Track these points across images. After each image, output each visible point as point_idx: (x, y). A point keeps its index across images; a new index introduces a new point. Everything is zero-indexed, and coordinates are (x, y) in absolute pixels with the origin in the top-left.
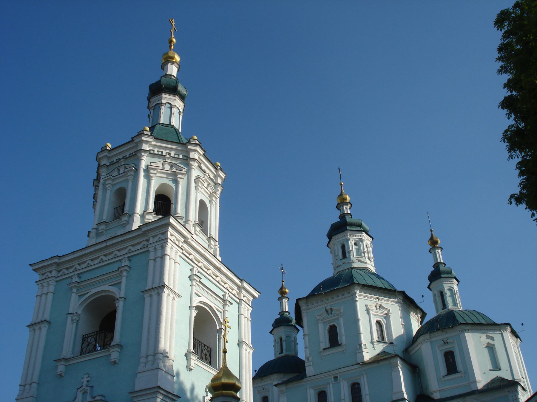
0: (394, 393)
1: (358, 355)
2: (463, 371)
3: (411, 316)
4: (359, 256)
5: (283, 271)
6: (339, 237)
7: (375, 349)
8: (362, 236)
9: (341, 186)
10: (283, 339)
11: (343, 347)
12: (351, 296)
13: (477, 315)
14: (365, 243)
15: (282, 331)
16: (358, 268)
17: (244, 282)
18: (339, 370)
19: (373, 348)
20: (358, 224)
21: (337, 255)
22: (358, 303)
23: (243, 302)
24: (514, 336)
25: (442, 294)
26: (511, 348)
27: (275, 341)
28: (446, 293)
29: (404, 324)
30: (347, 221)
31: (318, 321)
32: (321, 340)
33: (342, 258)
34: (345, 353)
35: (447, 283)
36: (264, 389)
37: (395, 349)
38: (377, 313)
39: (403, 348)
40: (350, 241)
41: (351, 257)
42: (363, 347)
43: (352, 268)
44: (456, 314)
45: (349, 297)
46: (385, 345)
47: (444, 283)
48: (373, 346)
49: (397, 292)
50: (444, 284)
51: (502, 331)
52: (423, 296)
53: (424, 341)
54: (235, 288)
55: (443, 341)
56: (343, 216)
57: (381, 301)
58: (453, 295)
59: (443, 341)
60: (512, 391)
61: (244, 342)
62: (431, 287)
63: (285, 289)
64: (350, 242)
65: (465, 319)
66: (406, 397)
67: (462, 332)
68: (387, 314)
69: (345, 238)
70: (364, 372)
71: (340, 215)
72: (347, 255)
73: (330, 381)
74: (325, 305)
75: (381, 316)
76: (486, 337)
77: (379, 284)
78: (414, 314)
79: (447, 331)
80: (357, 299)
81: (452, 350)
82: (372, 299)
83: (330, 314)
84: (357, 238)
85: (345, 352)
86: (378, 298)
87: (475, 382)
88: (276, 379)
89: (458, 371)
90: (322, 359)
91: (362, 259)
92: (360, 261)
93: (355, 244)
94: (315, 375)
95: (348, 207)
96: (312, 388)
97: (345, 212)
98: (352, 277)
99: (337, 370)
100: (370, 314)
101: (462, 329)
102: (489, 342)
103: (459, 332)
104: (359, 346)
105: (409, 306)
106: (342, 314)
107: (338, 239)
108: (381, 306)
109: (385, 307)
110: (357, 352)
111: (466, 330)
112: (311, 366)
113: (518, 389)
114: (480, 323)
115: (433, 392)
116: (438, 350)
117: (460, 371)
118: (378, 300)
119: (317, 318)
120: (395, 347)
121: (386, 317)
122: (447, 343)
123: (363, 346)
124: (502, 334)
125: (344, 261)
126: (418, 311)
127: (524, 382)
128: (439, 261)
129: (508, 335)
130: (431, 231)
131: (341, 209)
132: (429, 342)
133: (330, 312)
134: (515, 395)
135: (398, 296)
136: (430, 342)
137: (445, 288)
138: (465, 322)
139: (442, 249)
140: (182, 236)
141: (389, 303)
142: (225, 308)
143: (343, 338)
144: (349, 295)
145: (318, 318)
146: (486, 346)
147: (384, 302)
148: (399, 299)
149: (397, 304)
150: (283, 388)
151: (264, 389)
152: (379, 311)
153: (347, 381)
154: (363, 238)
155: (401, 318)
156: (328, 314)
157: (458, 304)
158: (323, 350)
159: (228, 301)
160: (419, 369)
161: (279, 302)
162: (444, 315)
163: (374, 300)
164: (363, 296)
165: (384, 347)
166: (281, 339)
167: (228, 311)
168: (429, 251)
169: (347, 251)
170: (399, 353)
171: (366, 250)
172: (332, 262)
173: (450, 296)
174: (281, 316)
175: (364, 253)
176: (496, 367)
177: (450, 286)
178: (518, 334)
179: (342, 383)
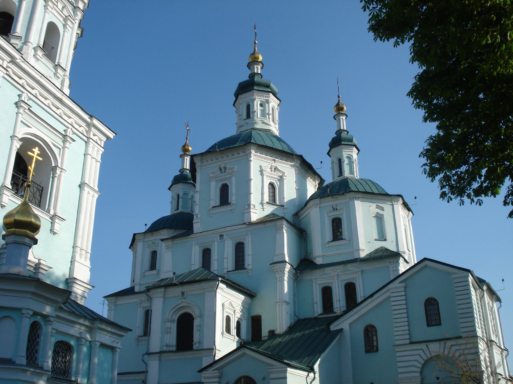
0: (276, 255)
1: (246, 215)
2: (348, 239)
3: (307, 181)
4: (264, 117)
5: (188, 128)
6: (246, 96)
7: (264, 210)
8: (269, 98)
9: (254, 45)
10: (180, 196)
11: (232, 206)
12: (245, 156)
13: (371, 185)
14: (271, 105)
15: (180, 188)
16: (260, 129)
17: (94, 118)
18: (225, 228)
19: (262, 209)
20: (266, 85)
21: (241, 115)
22: (252, 164)
23: (91, 140)
24: (406, 209)
25: (340, 161)
26: (400, 219)
27: (172, 197)
28: (344, 161)
29: (298, 188)
30: (255, 80)
32: (212, 198)
34: (233, 212)
35: (346, 150)
36: (154, 243)
37: (284, 212)
38: (271, 174)
39: (294, 212)
40: (256, 101)
42: (251, 208)
43: (254, 129)
44: (349, 181)
46: (276, 207)
47: (343, 150)
48: (262, 207)
49: (294, 155)
50: (343, 152)
51: (393, 202)
52: (321, 162)
53: (313, 206)
54: (84, 124)
55: (332, 207)
56: (252, 76)
57: (277, 163)
58: (351, 163)
59: (332, 207)
60: (393, 262)
61: (86, 184)
62: (330, 154)
63: (188, 146)
65: (358, 187)
66: (287, 259)
68: (281, 177)
69: (251, 98)
70: (249, 232)
71: (250, 74)
72: (251, 115)
73: (216, 239)
74: (220, 163)
76: (376, 206)
77: (278, 146)
78: (312, 180)
79: (337, 198)
80: (252, 159)
81: (340, 216)
82: (268, 160)
84: (263, 99)
85: (234, 211)
86: (274, 160)
87: (359, 250)
88: (166, 234)
89: (343, 239)
90: (211, 217)
92: (263, 123)
93: (261, 105)
94: (201, 232)
95: (259, 67)
96: (197, 245)
97: (255, 72)
98: (250, 136)
99: (223, 229)
100: (264, 175)
101: (353, 197)
102: (379, 212)
104: (248, 206)
105: (307, 171)
107: (244, 98)
108: (276, 168)
109: (281, 170)
110: (245, 212)
111: (357, 198)
112: (199, 223)
113: (399, 260)
114: (372, 192)
115: (316, 257)
116: (325, 215)
117: (345, 238)
118: (274, 162)
119: (211, 176)
120: (285, 210)
121: (280, 179)
122: (336, 209)
123: (252, 207)
124: (393, 205)
125: (247, 121)
127: (409, 254)
128: (342, 128)
129: (399, 207)
130: (339, 97)
131: (252, 69)
132: (319, 207)
133: (223, 170)
134: (396, 267)
135: (295, 160)
136: (320, 207)
138: (357, 190)
139: (347, 116)
140: (9, 56)
141: (286, 166)
142: (65, 144)
143: (233, 198)
144: (245, 154)
145: (211, 175)
146: (375, 216)
147: (280, 164)
148: (296, 162)
149: (294, 167)
150: (170, 243)
151: (154, 243)
152: (274, 173)
153: (232, 240)
154: (269, 100)
155: (296, 182)
156: (222, 173)
157: (355, 173)
158: (212, 207)
159: (68, 137)
160: (306, 234)
161: (181, 159)
162: (338, 182)
163: (270, 161)
165: (274, 209)
166: (178, 196)
167: (68, 149)
168: (334, 117)
169: (252, 111)
170: (289, 217)
171: (271, 112)
172: (236, 122)
173: (347, 164)
174: (181, 173)
175: (269, 114)
176: (382, 237)
177: (350, 154)
178: (410, 207)
179: (226, 241)
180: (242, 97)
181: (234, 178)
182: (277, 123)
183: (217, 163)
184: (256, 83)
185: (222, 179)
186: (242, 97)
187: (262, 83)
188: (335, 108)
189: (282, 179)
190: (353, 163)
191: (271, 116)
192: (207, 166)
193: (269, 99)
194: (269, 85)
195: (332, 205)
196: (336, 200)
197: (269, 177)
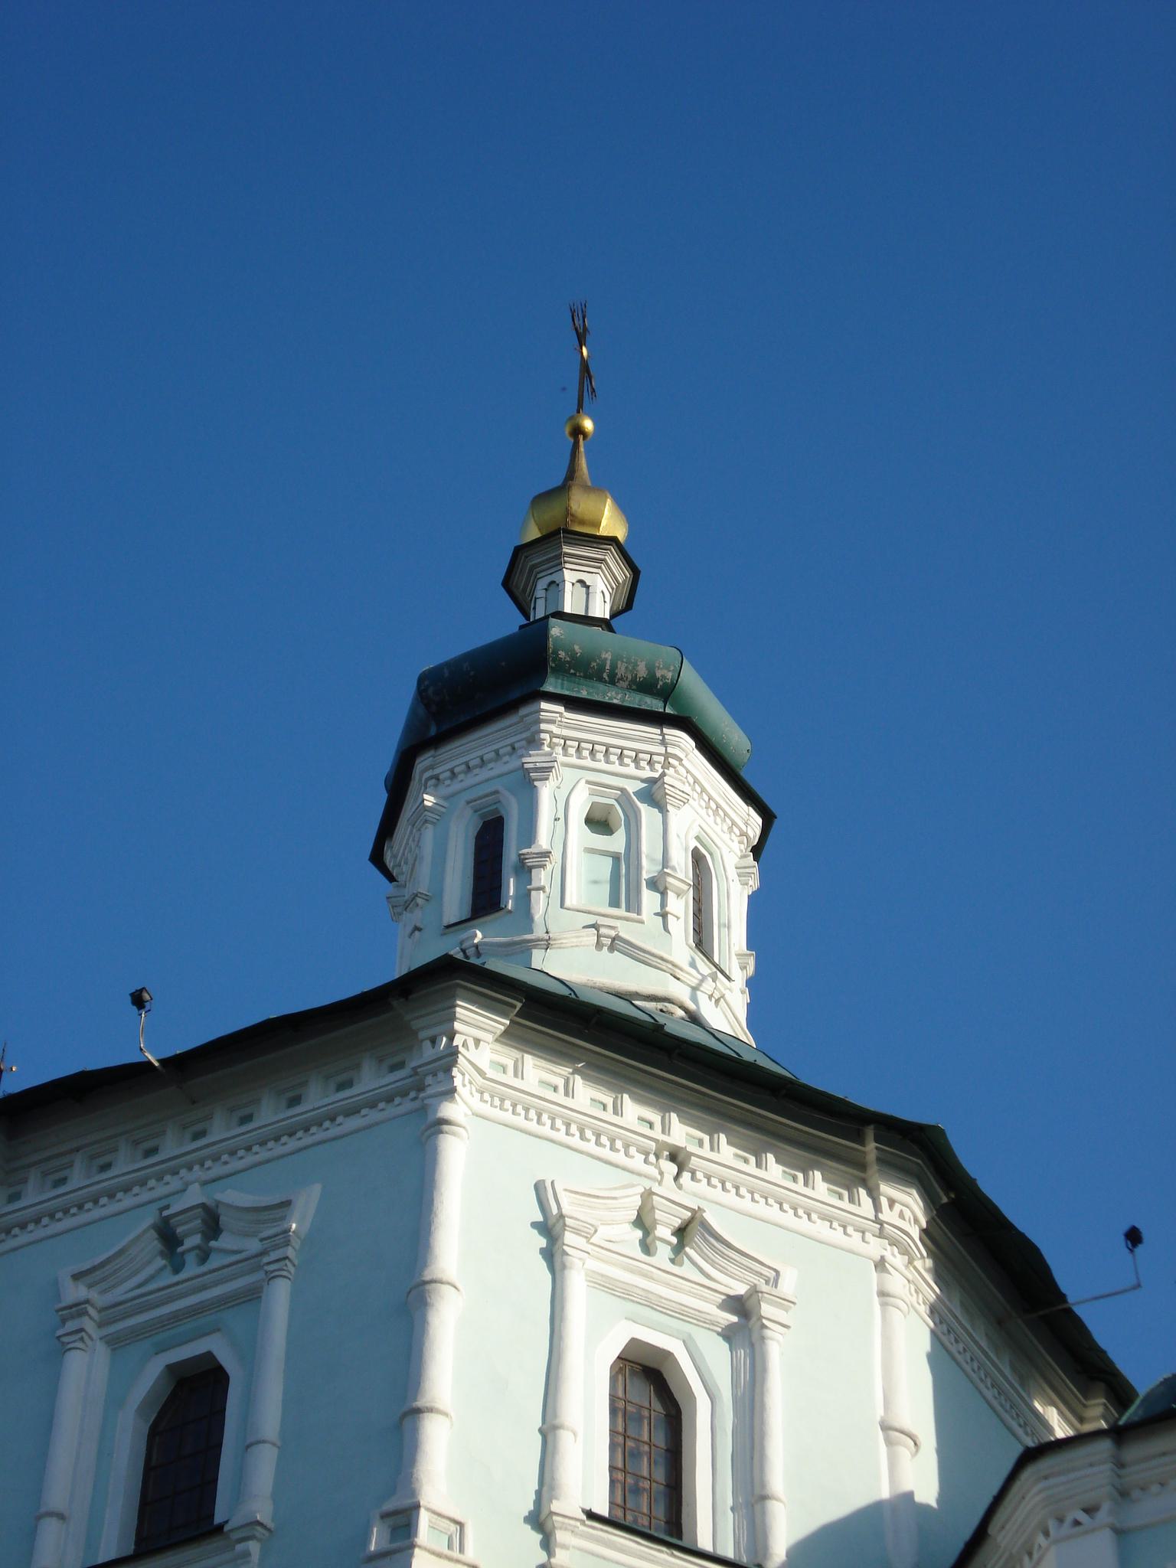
6: (473, 758)
8: (666, 765)
11: (239, 1547)
12: (404, 1094)
20: (642, 672)
31: (71, 1326)
32: (57, 1497)
33: (466, 913)
41: (540, 904)
45: (389, 1099)
53: (1052, 1524)
64: (546, 793)
68: (742, 1307)
69: (514, 764)
75: (682, 1314)
83: (191, 1259)
86: (676, 1156)
91: (626, 930)
92: (616, 944)
93: (598, 823)
97: (568, 609)
106: (290, 1252)
126: (1099, 1410)
133: (193, 1241)
136: (1119, 1532)
141: (788, 1218)
145: (76, 1292)
147: (730, 1198)
154: (666, 779)
163: (637, 1161)
164: (524, 1102)
175: (657, 885)
180: (437, 771)
181: (280, 1296)
182: (740, 977)
183: (143, 1183)
184: (562, 654)
185: (176, 1317)
186: (437, 771)
187: (608, 656)
189: (754, 1319)
191: (680, 906)
192: (45, 1220)
193: (663, 775)
194: (669, 675)
197: (624, 1293)
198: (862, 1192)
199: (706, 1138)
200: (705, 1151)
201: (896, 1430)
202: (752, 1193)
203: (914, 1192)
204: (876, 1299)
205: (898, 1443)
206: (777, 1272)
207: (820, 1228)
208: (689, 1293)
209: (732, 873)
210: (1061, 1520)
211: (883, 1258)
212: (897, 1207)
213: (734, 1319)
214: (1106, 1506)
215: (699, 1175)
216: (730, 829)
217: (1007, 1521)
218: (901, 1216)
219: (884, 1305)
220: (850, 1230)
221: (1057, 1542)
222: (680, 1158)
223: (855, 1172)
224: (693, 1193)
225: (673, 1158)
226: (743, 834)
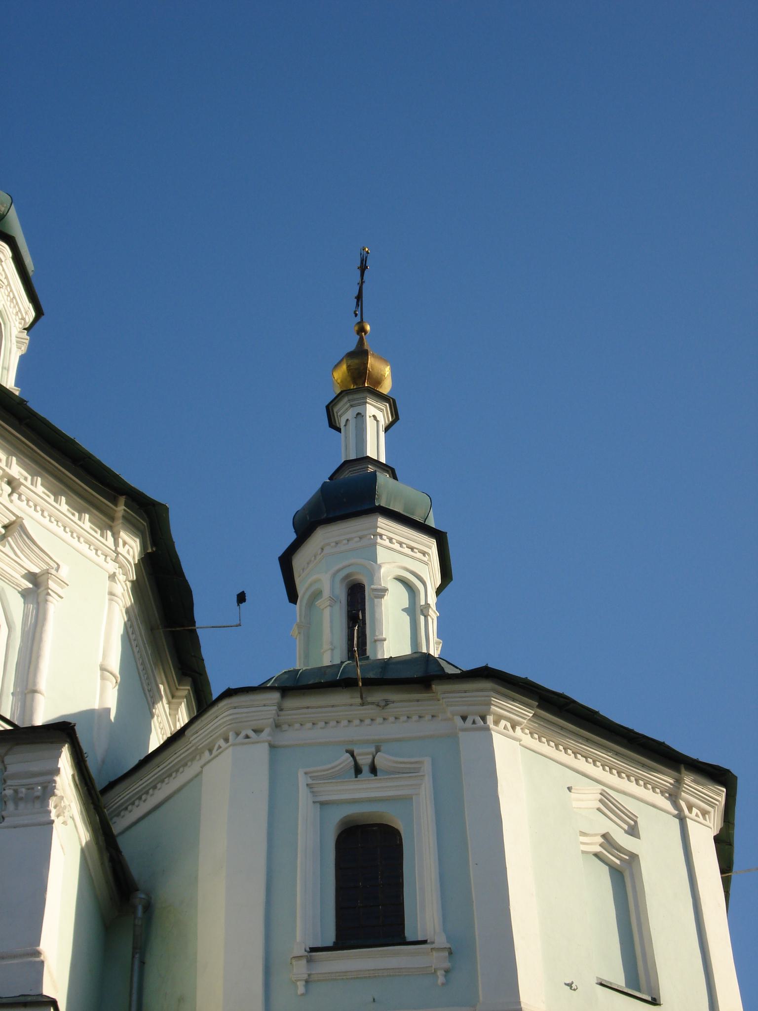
53: (231, 736)
55: (348, 755)
67: (474, 722)
79: (387, 703)
103: (458, 721)
116: (304, 796)
121: (28, 589)
122: (373, 770)
126: (186, 693)
130: (361, 330)
132: (266, 746)
136: (272, 747)
137: (380, 567)
141: (67, 536)
147: (38, 516)
160: (148, 907)
188: (344, 367)
189: (42, 589)
190: (426, 617)
195: (352, 742)
196: (379, 720)
198: (109, 533)
199: (29, 478)
200: (28, 484)
201: (108, 672)
202: (50, 516)
203: (138, 540)
204: (107, 597)
205: (107, 680)
206: (58, 566)
207: (84, 547)
208: (8, 565)
209: (14, 340)
210: (238, 734)
211: (115, 573)
212: (127, 547)
213: (31, 586)
214: (267, 731)
215: (23, 498)
216: (17, 314)
217: (201, 729)
218: (128, 552)
219: (111, 600)
220: (99, 552)
221: (233, 745)
222: (14, 484)
223: (107, 520)
224: (19, 507)
225: (9, 483)
226: (23, 319)
